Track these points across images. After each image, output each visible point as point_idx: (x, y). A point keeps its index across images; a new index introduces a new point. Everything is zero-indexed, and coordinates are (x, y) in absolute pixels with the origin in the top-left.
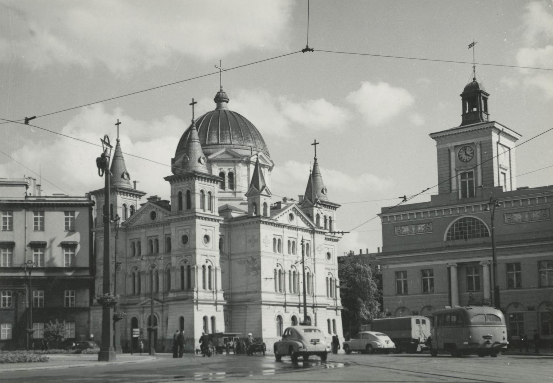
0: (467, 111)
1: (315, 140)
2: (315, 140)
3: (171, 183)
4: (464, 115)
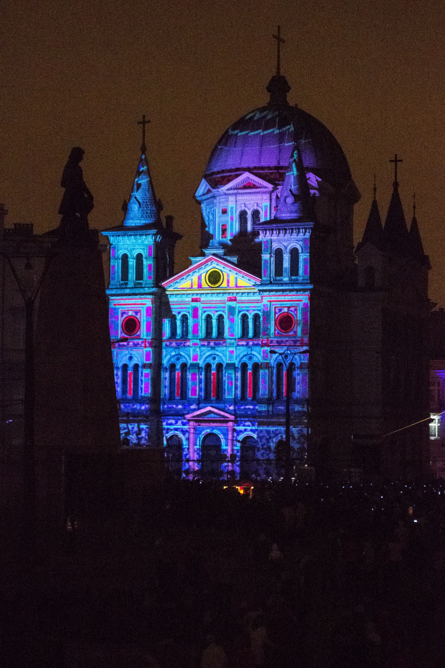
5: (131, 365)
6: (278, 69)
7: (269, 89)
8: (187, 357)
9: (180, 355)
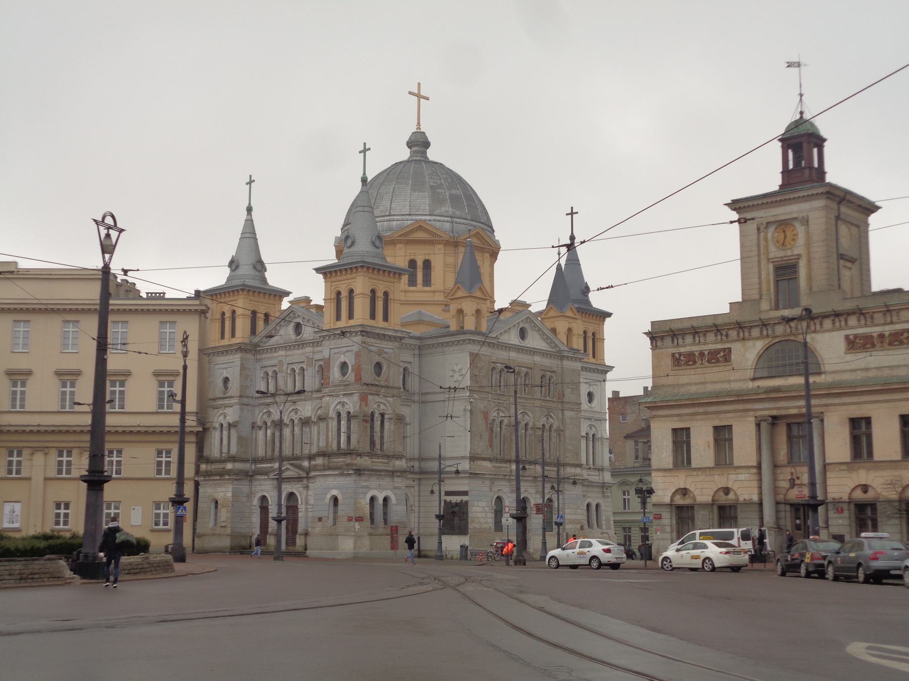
0: (791, 166)
1: (572, 208)
2: (572, 208)
3: (325, 278)
4: (785, 172)
5: (225, 425)
6: (419, 123)
7: (410, 144)
8: (274, 413)
9: (270, 411)
